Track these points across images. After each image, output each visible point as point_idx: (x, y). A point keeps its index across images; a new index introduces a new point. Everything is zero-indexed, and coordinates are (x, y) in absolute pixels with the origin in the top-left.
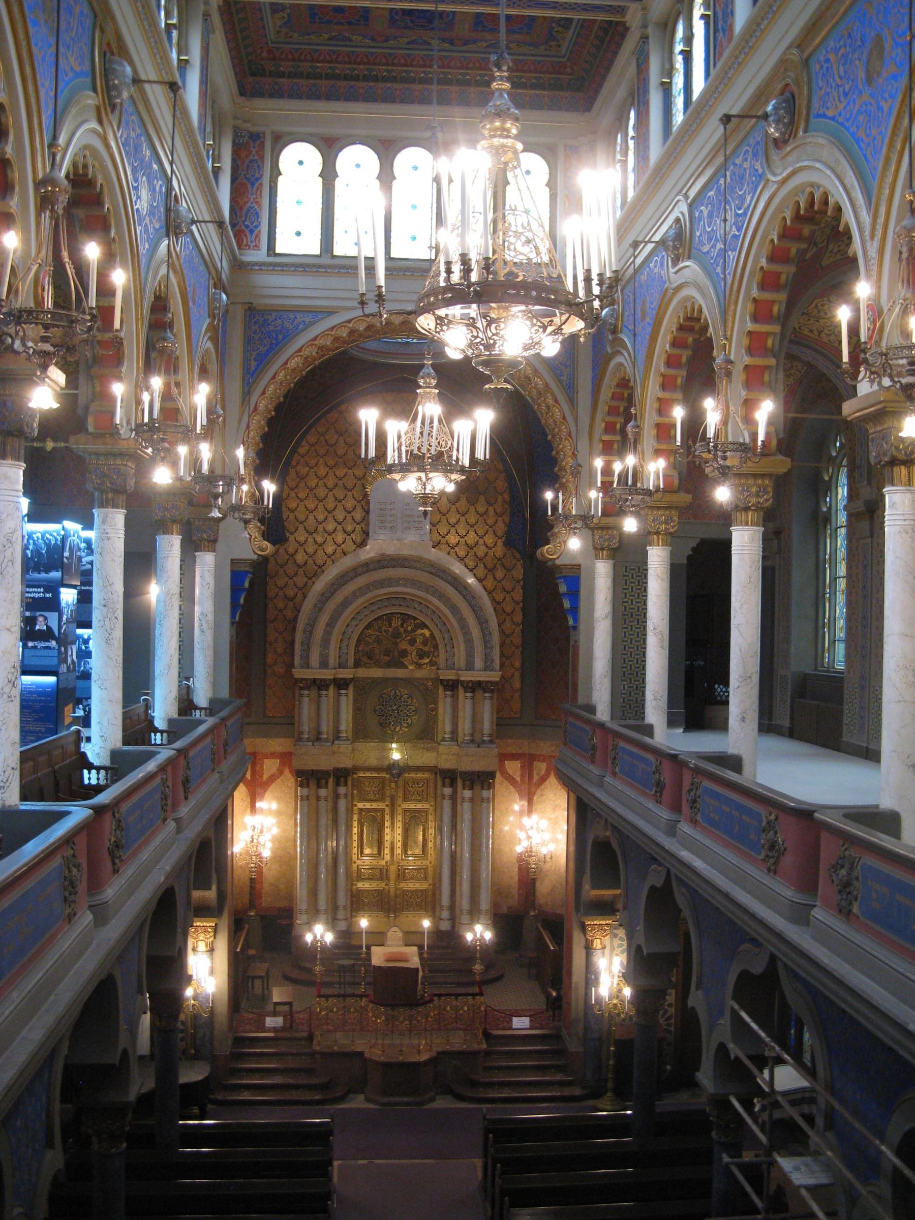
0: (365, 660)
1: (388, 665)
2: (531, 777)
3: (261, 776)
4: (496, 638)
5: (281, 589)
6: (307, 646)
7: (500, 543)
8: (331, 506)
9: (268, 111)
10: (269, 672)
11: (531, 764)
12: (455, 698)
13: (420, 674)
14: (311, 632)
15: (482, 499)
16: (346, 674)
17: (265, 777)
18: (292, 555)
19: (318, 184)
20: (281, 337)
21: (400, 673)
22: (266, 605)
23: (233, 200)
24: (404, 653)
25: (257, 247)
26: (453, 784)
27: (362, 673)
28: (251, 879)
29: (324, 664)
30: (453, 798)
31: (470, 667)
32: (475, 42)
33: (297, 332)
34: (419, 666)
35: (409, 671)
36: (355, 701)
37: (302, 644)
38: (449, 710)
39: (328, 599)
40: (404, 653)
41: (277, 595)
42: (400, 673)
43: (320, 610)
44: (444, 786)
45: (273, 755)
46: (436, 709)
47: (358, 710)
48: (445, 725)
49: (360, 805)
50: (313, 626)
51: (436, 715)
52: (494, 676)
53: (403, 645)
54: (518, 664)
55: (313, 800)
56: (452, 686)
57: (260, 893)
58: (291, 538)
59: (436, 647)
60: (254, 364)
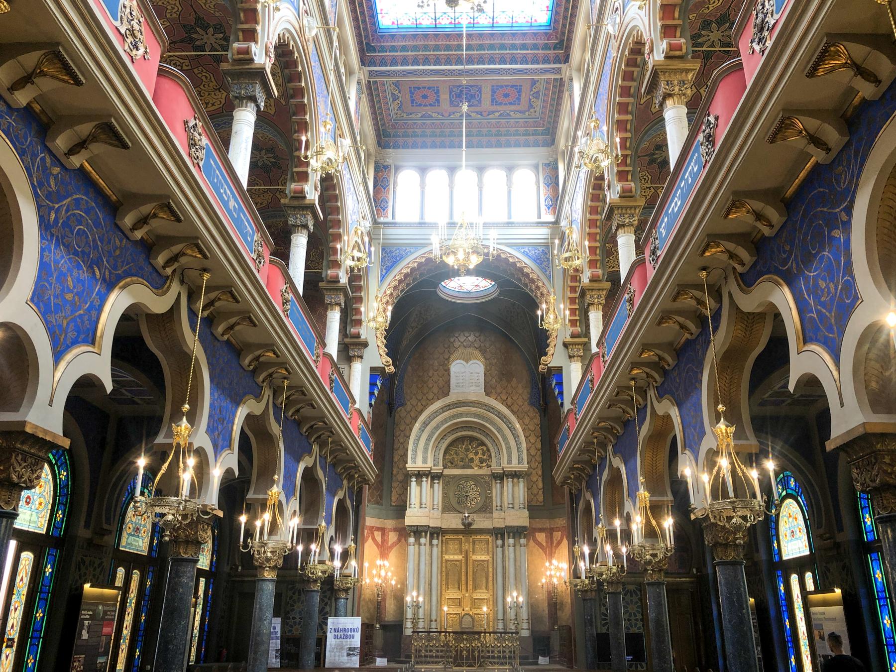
0: (449, 464)
1: (463, 467)
2: (552, 543)
4: (524, 445)
7: (526, 403)
9: (392, 156)
11: (551, 534)
12: (502, 484)
13: (481, 472)
15: (514, 380)
16: (438, 469)
17: (390, 543)
19: (419, 189)
21: (469, 472)
23: (375, 187)
24: (472, 460)
25: (387, 217)
26: (503, 539)
27: (447, 472)
29: (425, 461)
30: (503, 546)
31: (510, 462)
32: (493, 112)
33: (407, 255)
34: (481, 468)
35: (475, 471)
36: (443, 488)
38: (499, 492)
40: (472, 460)
42: (469, 472)
44: (497, 539)
46: (491, 493)
47: (445, 496)
48: (496, 500)
49: (447, 557)
51: (491, 497)
52: (524, 467)
53: (471, 456)
54: (540, 473)
55: (417, 546)
56: (500, 477)
58: (408, 403)
59: (490, 456)
60: (384, 271)
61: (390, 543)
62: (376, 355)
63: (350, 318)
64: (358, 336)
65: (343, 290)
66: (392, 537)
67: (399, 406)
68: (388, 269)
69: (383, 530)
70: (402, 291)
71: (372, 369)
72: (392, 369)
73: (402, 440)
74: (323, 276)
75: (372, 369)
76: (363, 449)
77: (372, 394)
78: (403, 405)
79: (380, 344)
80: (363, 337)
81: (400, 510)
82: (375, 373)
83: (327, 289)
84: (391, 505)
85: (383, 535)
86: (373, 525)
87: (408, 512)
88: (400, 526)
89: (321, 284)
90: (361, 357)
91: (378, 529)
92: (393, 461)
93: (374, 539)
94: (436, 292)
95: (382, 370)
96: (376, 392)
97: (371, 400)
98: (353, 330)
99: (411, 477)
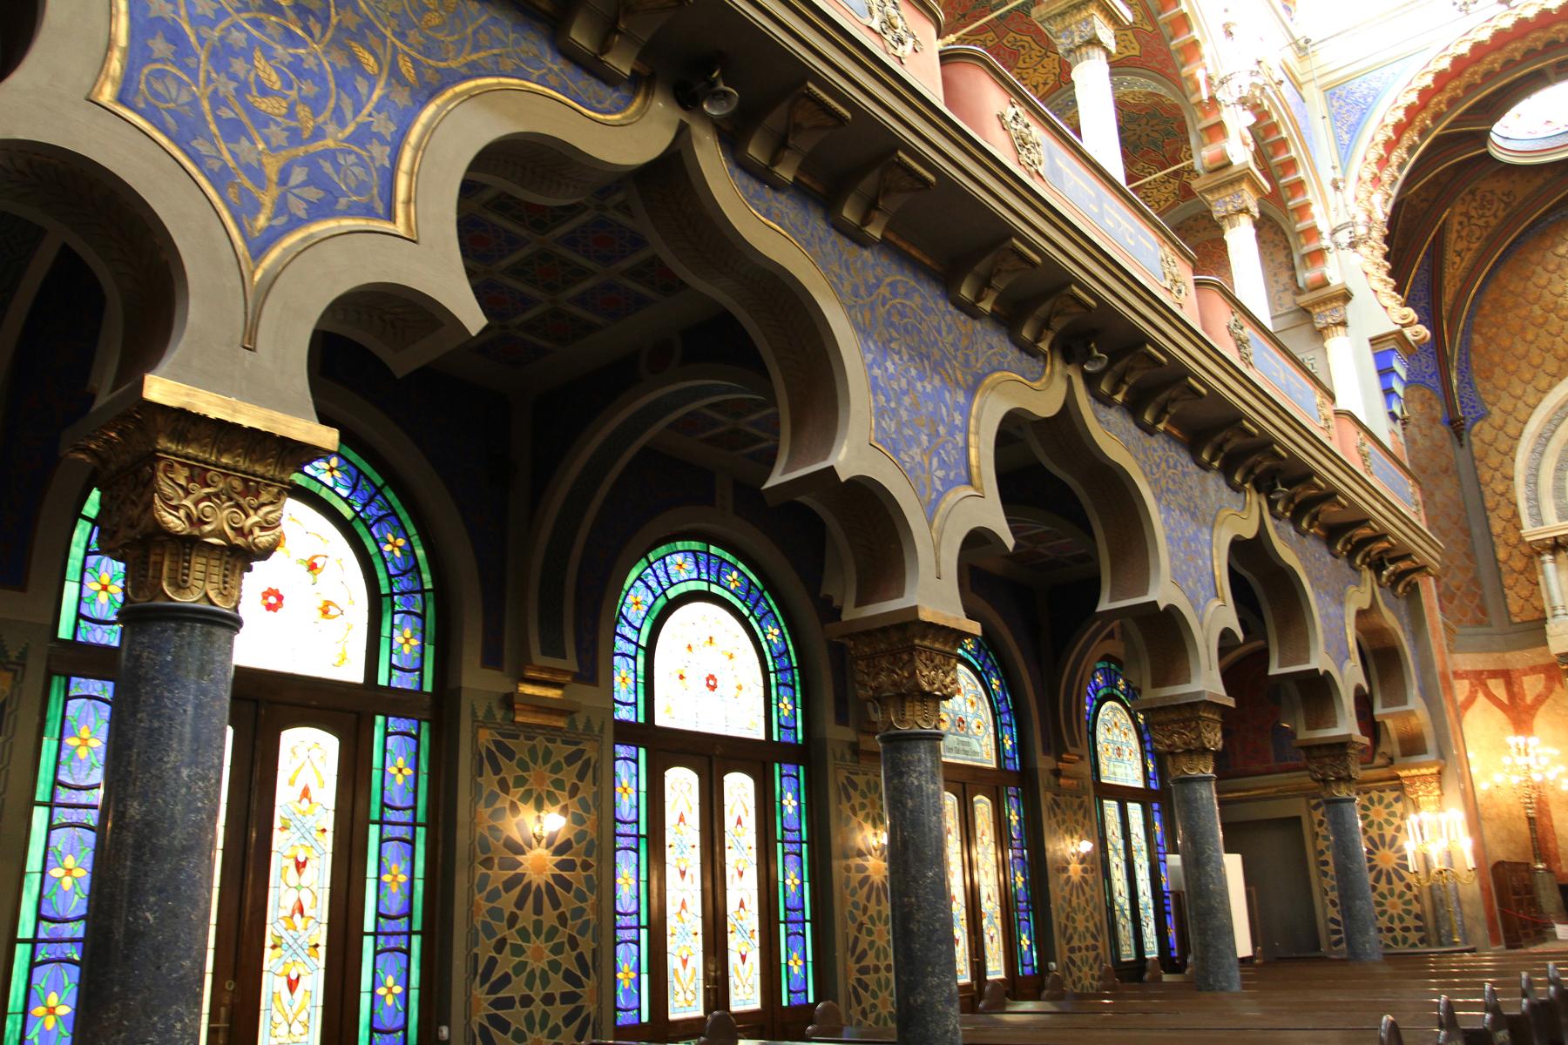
3: (1523, 698)
5: (1496, 469)
6: (1534, 500)
8: (1537, 361)
10: (1504, 568)
14: (1536, 484)
17: (1529, 699)
18: (1501, 428)
20: (1370, 100)
22: (1481, 493)
28: (1530, 819)
37: (1528, 499)
39: (1548, 440)
41: (1493, 478)
43: (1541, 454)
45: (1534, 670)
50: (1536, 476)
57: (1557, 855)
58: (1495, 410)
60: (1346, 137)
61: (1529, 699)
62: (1377, 307)
63: (1281, 233)
64: (1325, 283)
65: (1245, 176)
66: (1532, 686)
67: (1476, 420)
68: (1354, 129)
69: (1506, 676)
70: (1401, 167)
71: (1374, 341)
72: (1424, 332)
73: (1501, 488)
74: (1197, 167)
75: (1374, 341)
76: (1394, 497)
77: (1388, 392)
78: (1483, 416)
79: (1379, 286)
80: (1334, 282)
81: (1536, 629)
82: (1384, 348)
83: (1211, 191)
84: (1511, 623)
85: (1509, 685)
86: (1480, 667)
87: (1552, 627)
88: (1541, 661)
89: (1196, 185)
90: (1344, 324)
91: (1494, 674)
92: (1491, 534)
93: (1489, 696)
94: (1488, 156)
95: (1399, 337)
96: (1398, 387)
97: (1389, 405)
98: (1306, 276)
99: (1539, 554)
